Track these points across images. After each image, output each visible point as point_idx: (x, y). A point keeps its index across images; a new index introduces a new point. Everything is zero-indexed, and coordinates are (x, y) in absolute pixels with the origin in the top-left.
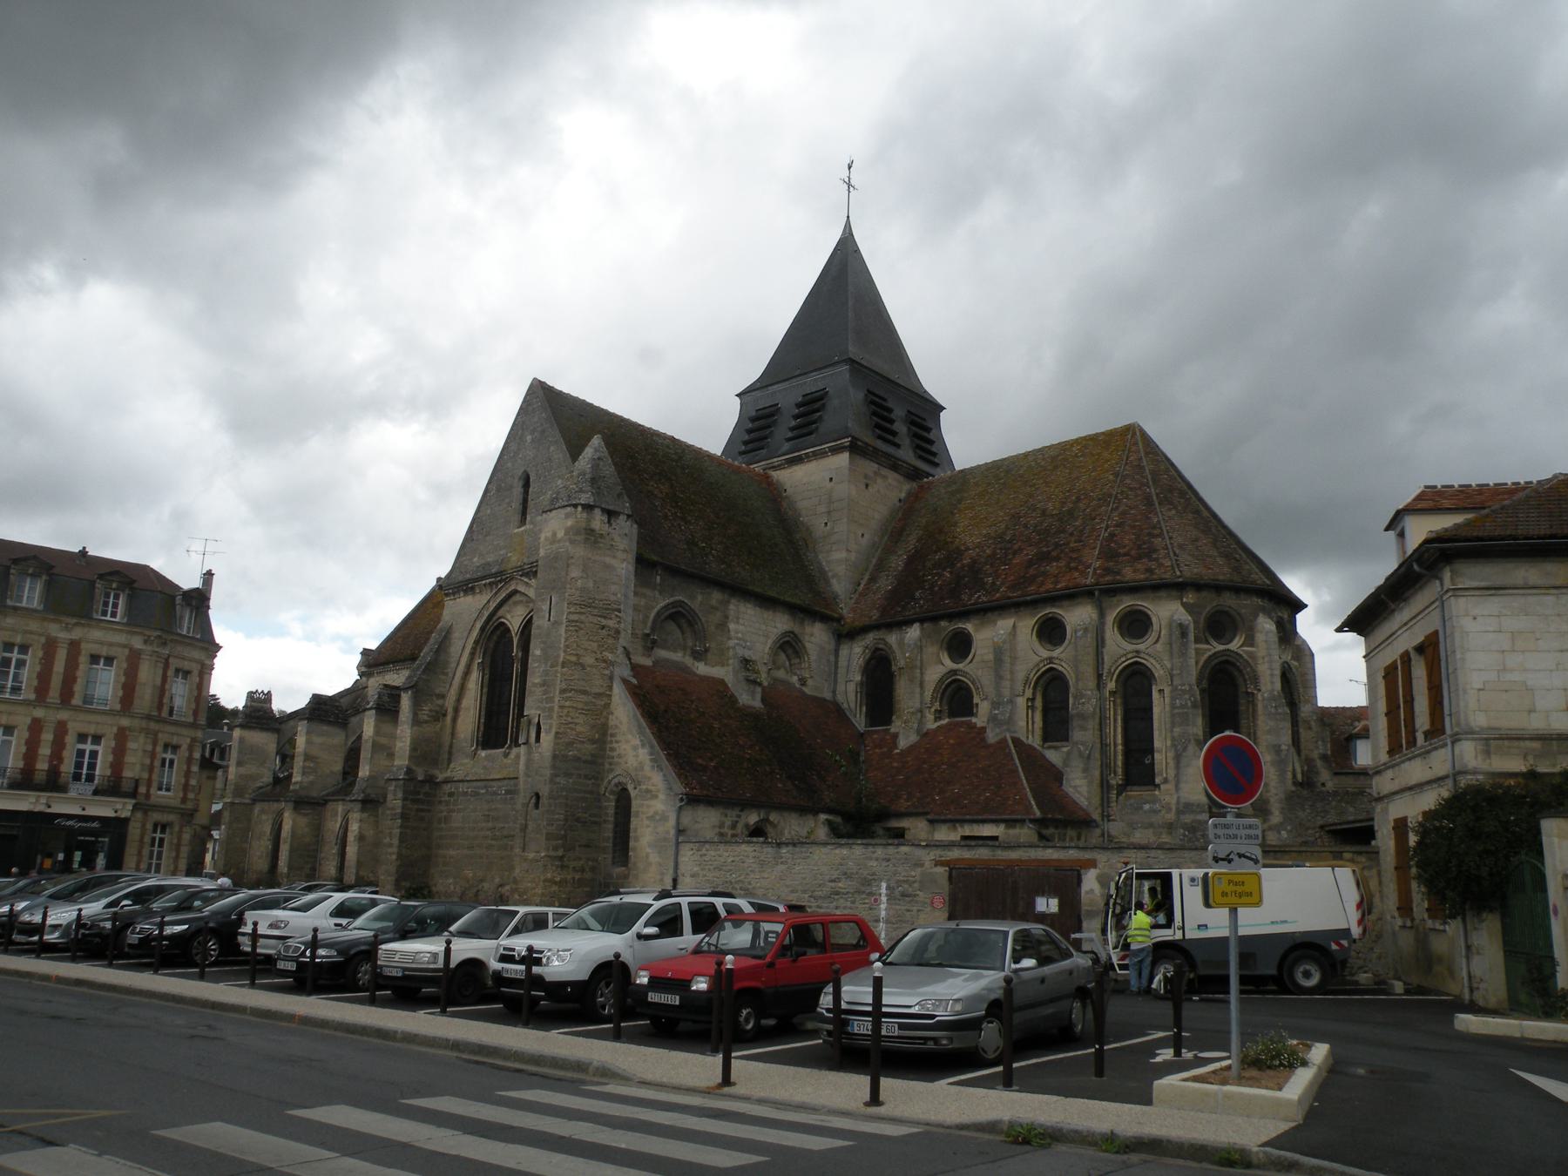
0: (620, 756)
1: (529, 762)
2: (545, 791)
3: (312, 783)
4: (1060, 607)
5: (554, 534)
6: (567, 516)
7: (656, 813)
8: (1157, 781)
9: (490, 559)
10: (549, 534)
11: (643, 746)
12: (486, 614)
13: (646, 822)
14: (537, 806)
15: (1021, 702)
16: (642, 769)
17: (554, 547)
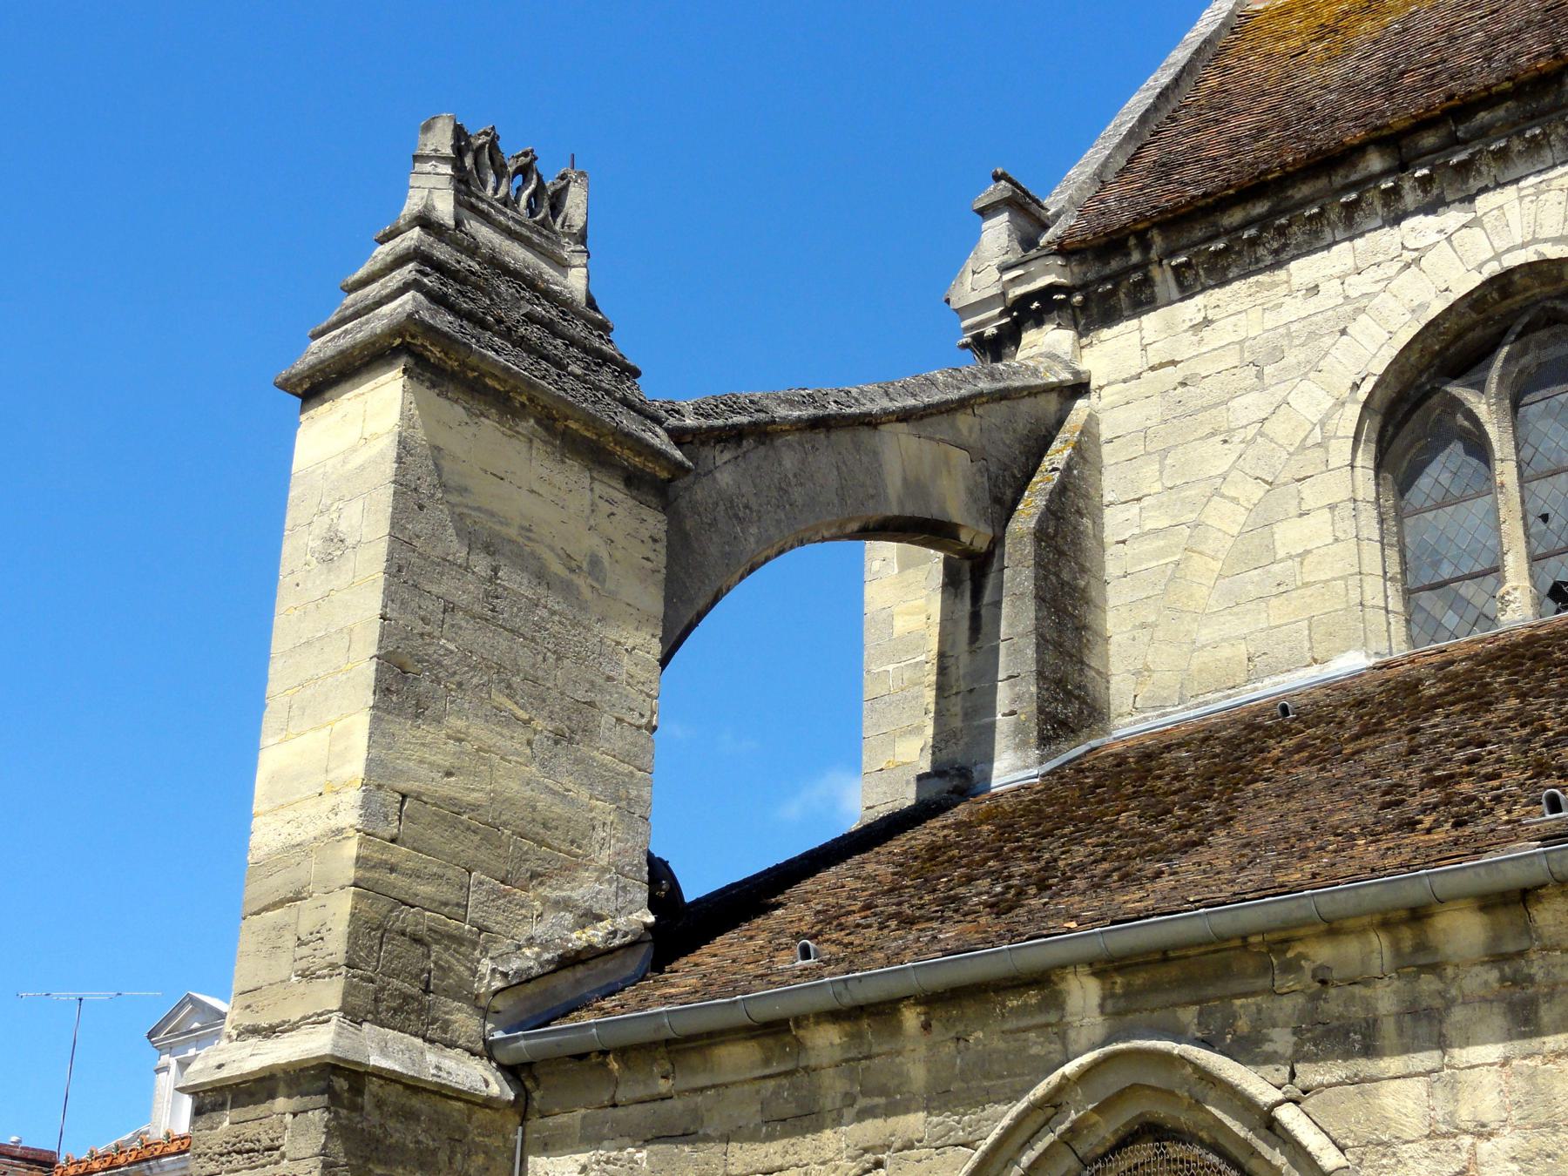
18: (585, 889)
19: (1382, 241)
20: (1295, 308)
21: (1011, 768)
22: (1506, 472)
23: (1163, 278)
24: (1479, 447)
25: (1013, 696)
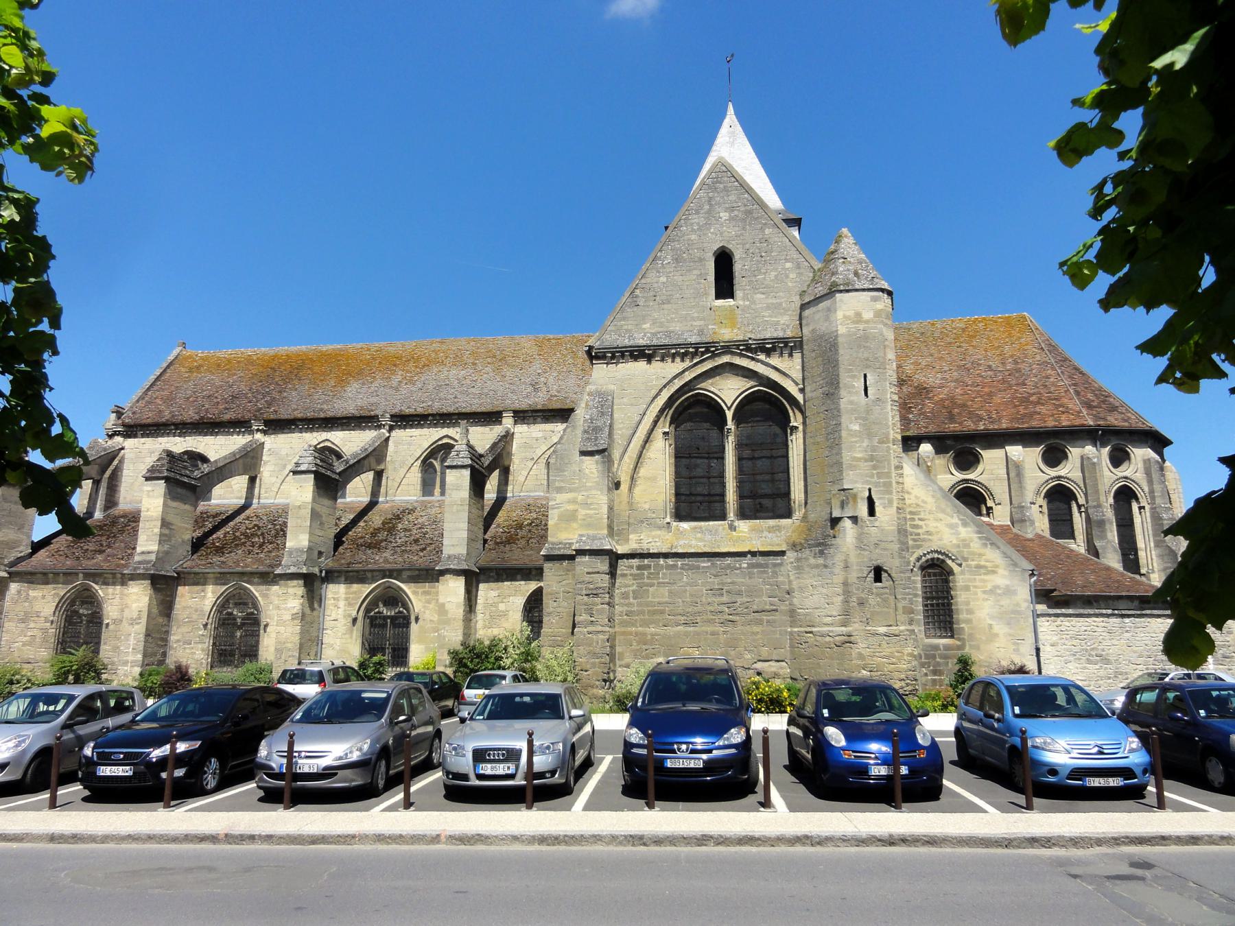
1: (860, 538)
2: (891, 564)
3: (167, 553)
4: (1064, 440)
5: (858, 314)
6: (875, 299)
7: (998, 587)
8: (1143, 571)
9: (676, 327)
10: (851, 313)
11: (965, 524)
12: (678, 384)
13: (980, 595)
14: (878, 579)
15: (1035, 508)
16: (967, 546)
17: (861, 327)
18: (22, 548)
19: (171, 439)
21: (98, 515)
25: (100, 504)
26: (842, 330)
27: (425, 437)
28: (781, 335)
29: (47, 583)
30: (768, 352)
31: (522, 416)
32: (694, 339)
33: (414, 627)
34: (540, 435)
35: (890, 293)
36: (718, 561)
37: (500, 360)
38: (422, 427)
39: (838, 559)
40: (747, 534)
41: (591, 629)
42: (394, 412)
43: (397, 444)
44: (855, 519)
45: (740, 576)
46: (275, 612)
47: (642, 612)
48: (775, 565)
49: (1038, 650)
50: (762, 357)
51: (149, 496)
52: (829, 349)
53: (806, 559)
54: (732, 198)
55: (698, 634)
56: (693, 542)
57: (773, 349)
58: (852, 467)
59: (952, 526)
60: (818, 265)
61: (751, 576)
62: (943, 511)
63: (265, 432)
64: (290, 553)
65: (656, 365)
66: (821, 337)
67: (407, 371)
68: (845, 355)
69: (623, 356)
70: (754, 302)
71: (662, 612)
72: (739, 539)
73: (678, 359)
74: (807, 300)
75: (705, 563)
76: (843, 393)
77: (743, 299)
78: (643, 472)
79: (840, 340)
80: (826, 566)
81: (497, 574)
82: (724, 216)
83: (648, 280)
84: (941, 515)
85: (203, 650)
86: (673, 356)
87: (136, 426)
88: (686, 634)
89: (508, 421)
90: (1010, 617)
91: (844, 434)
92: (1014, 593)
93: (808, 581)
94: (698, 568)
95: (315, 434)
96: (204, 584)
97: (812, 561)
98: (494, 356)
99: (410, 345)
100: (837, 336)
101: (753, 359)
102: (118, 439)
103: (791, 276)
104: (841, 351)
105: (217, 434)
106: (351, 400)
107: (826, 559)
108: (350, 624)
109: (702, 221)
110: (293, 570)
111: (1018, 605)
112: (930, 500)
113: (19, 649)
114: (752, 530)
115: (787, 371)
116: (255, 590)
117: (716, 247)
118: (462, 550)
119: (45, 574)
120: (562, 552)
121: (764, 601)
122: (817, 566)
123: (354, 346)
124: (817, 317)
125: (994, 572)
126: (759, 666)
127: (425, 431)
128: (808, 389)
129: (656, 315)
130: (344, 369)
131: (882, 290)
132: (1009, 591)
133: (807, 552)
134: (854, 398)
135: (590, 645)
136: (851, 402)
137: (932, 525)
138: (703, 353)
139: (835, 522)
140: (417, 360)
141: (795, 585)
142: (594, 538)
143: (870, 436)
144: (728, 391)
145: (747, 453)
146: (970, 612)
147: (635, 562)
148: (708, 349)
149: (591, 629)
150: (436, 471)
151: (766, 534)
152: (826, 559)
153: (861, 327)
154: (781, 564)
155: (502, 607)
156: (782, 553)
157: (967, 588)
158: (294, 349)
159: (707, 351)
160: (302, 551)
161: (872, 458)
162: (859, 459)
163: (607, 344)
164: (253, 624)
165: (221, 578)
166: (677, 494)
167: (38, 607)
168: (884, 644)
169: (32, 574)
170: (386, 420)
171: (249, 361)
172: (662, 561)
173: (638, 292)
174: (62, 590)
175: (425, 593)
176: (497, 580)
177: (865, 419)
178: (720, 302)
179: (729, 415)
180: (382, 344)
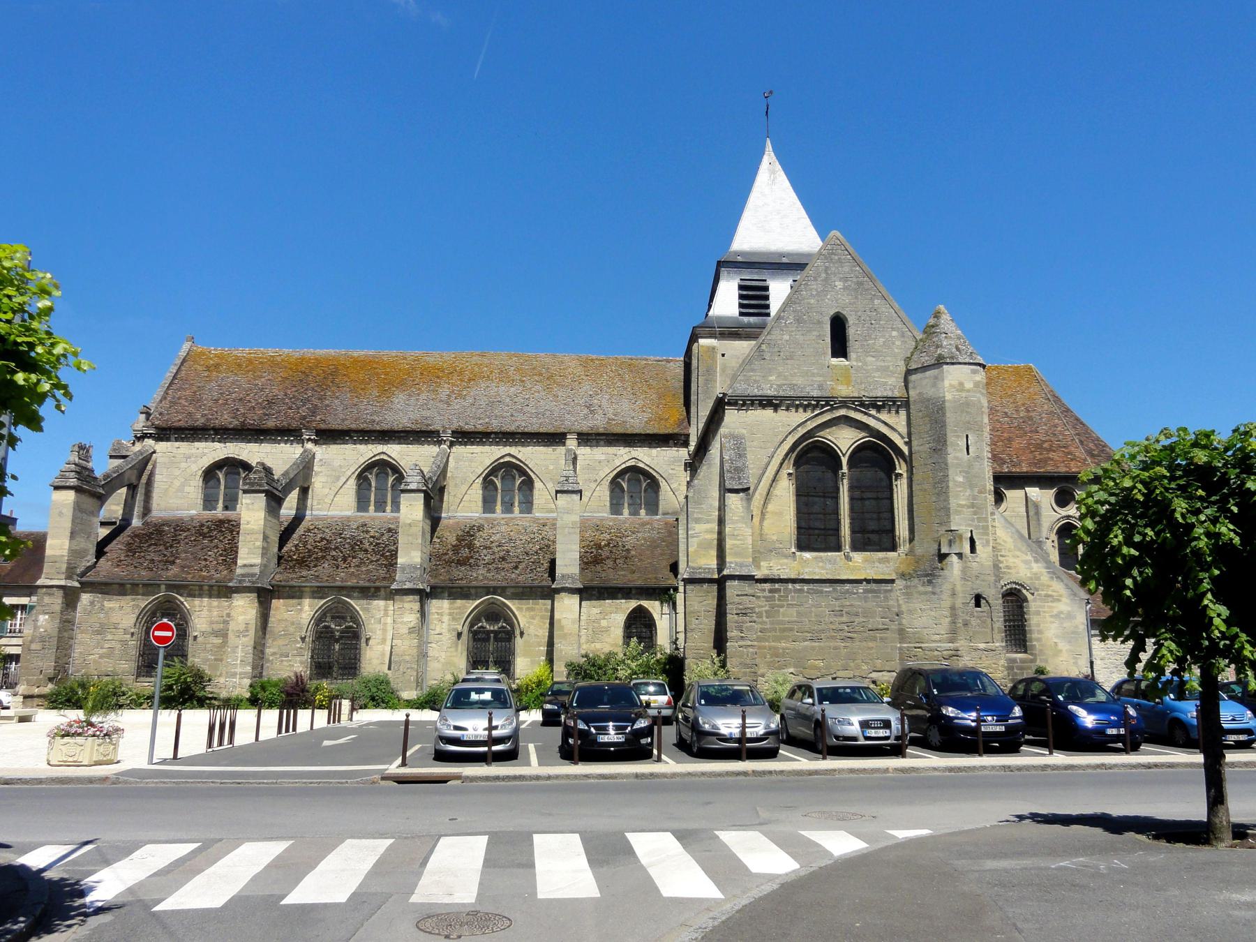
0: (1008, 567)
1: (964, 570)
5: (961, 384)
6: (974, 372)
9: (799, 381)
10: (955, 383)
11: (1037, 561)
12: (801, 431)
14: (978, 605)
16: (1038, 579)
17: (964, 394)
19: (210, 444)
20: (194, 451)
21: (136, 522)
22: (222, 487)
23: (172, 438)
24: (219, 480)
25: (137, 510)
26: (948, 397)
27: (488, 455)
28: (890, 394)
29: (124, 594)
30: (879, 409)
31: (587, 438)
32: (815, 393)
33: (519, 642)
34: (603, 457)
35: (984, 367)
36: (839, 587)
37: (549, 379)
38: (483, 444)
39: (946, 587)
40: (862, 564)
41: (741, 643)
42: (454, 427)
43: (457, 460)
44: (960, 555)
45: (856, 599)
46: (378, 626)
47: (775, 630)
48: (886, 591)
49: (1092, 663)
50: (873, 412)
51: (248, 509)
52: (936, 413)
53: (915, 587)
54: (846, 269)
55: (821, 648)
56: (817, 570)
57: (883, 406)
58: (958, 513)
59: (1026, 562)
60: (920, 336)
61: (866, 599)
62: (1019, 550)
63: (316, 442)
64: (403, 569)
65: (782, 413)
66: (928, 400)
67: (453, 385)
68: (950, 418)
69: (752, 404)
70: (865, 364)
71: (791, 630)
72: (854, 569)
73: (801, 410)
74: (914, 367)
75: (827, 588)
76: (950, 450)
77: (858, 360)
78: (770, 507)
79: (947, 404)
80: (934, 593)
81: (599, 592)
82: (839, 285)
83: (773, 337)
84: (1018, 553)
85: (301, 663)
86: (797, 407)
87: (170, 429)
88: (813, 648)
89: (572, 442)
90: (1071, 636)
91: (951, 484)
92: (1074, 618)
93: (917, 604)
94: (822, 592)
95: (370, 446)
96: (300, 597)
97: (921, 589)
98: (541, 374)
99: (449, 356)
100: (944, 402)
101: (866, 414)
102: (149, 442)
103: (898, 343)
104: (948, 415)
105: (262, 442)
106: (402, 412)
107: (934, 587)
108: (455, 638)
109: (820, 288)
110: (408, 586)
111: (1076, 627)
112: (1009, 540)
113: (95, 661)
114: (866, 560)
115: (894, 425)
116: (357, 604)
117: (832, 312)
118: (575, 569)
119: (122, 585)
120: (702, 576)
121: (877, 621)
122: (925, 593)
123: (388, 354)
124: (924, 382)
125: (1059, 600)
126: (874, 675)
127: (487, 448)
128: (914, 443)
129: (781, 369)
130: (389, 379)
131: (980, 365)
132: (1070, 616)
133: (916, 581)
134: (958, 454)
135: (741, 657)
136: (957, 458)
137: (1011, 561)
138: (823, 406)
139: (942, 557)
140: (461, 373)
141: (904, 608)
142: (741, 565)
143: (972, 487)
144: (844, 440)
145: (857, 494)
146: (1040, 632)
147: (767, 586)
148: (828, 402)
149: (741, 643)
150: (496, 489)
151: (877, 564)
152: (934, 587)
153: (964, 394)
154: (891, 591)
155: (604, 623)
156: (892, 581)
157: (1038, 613)
158: (321, 352)
159: (827, 404)
160: (415, 568)
161: (973, 506)
162: (963, 506)
163: (739, 392)
164: (354, 636)
165: (318, 592)
166: (799, 528)
167: (115, 618)
168: (984, 658)
169: (106, 584)
170: (447, 436)
171: (273, 364)
172: (790, 586)
173: (764, 347)
174: (144, 602)
175: (528, 609)
176: (599, 598)
177: (967, 472)
178: (835, 361)
179: (844, 461)
180: (418, 353)
